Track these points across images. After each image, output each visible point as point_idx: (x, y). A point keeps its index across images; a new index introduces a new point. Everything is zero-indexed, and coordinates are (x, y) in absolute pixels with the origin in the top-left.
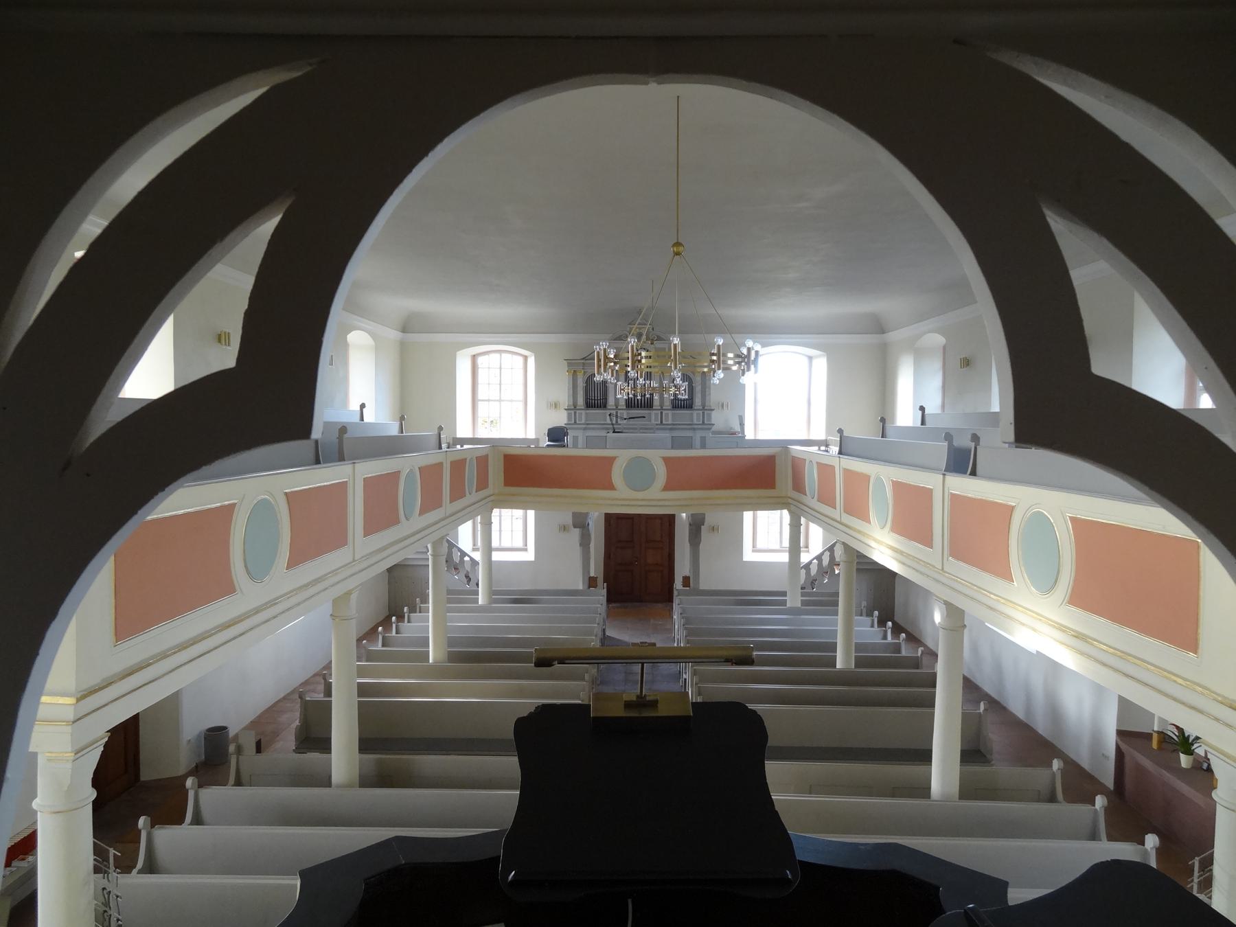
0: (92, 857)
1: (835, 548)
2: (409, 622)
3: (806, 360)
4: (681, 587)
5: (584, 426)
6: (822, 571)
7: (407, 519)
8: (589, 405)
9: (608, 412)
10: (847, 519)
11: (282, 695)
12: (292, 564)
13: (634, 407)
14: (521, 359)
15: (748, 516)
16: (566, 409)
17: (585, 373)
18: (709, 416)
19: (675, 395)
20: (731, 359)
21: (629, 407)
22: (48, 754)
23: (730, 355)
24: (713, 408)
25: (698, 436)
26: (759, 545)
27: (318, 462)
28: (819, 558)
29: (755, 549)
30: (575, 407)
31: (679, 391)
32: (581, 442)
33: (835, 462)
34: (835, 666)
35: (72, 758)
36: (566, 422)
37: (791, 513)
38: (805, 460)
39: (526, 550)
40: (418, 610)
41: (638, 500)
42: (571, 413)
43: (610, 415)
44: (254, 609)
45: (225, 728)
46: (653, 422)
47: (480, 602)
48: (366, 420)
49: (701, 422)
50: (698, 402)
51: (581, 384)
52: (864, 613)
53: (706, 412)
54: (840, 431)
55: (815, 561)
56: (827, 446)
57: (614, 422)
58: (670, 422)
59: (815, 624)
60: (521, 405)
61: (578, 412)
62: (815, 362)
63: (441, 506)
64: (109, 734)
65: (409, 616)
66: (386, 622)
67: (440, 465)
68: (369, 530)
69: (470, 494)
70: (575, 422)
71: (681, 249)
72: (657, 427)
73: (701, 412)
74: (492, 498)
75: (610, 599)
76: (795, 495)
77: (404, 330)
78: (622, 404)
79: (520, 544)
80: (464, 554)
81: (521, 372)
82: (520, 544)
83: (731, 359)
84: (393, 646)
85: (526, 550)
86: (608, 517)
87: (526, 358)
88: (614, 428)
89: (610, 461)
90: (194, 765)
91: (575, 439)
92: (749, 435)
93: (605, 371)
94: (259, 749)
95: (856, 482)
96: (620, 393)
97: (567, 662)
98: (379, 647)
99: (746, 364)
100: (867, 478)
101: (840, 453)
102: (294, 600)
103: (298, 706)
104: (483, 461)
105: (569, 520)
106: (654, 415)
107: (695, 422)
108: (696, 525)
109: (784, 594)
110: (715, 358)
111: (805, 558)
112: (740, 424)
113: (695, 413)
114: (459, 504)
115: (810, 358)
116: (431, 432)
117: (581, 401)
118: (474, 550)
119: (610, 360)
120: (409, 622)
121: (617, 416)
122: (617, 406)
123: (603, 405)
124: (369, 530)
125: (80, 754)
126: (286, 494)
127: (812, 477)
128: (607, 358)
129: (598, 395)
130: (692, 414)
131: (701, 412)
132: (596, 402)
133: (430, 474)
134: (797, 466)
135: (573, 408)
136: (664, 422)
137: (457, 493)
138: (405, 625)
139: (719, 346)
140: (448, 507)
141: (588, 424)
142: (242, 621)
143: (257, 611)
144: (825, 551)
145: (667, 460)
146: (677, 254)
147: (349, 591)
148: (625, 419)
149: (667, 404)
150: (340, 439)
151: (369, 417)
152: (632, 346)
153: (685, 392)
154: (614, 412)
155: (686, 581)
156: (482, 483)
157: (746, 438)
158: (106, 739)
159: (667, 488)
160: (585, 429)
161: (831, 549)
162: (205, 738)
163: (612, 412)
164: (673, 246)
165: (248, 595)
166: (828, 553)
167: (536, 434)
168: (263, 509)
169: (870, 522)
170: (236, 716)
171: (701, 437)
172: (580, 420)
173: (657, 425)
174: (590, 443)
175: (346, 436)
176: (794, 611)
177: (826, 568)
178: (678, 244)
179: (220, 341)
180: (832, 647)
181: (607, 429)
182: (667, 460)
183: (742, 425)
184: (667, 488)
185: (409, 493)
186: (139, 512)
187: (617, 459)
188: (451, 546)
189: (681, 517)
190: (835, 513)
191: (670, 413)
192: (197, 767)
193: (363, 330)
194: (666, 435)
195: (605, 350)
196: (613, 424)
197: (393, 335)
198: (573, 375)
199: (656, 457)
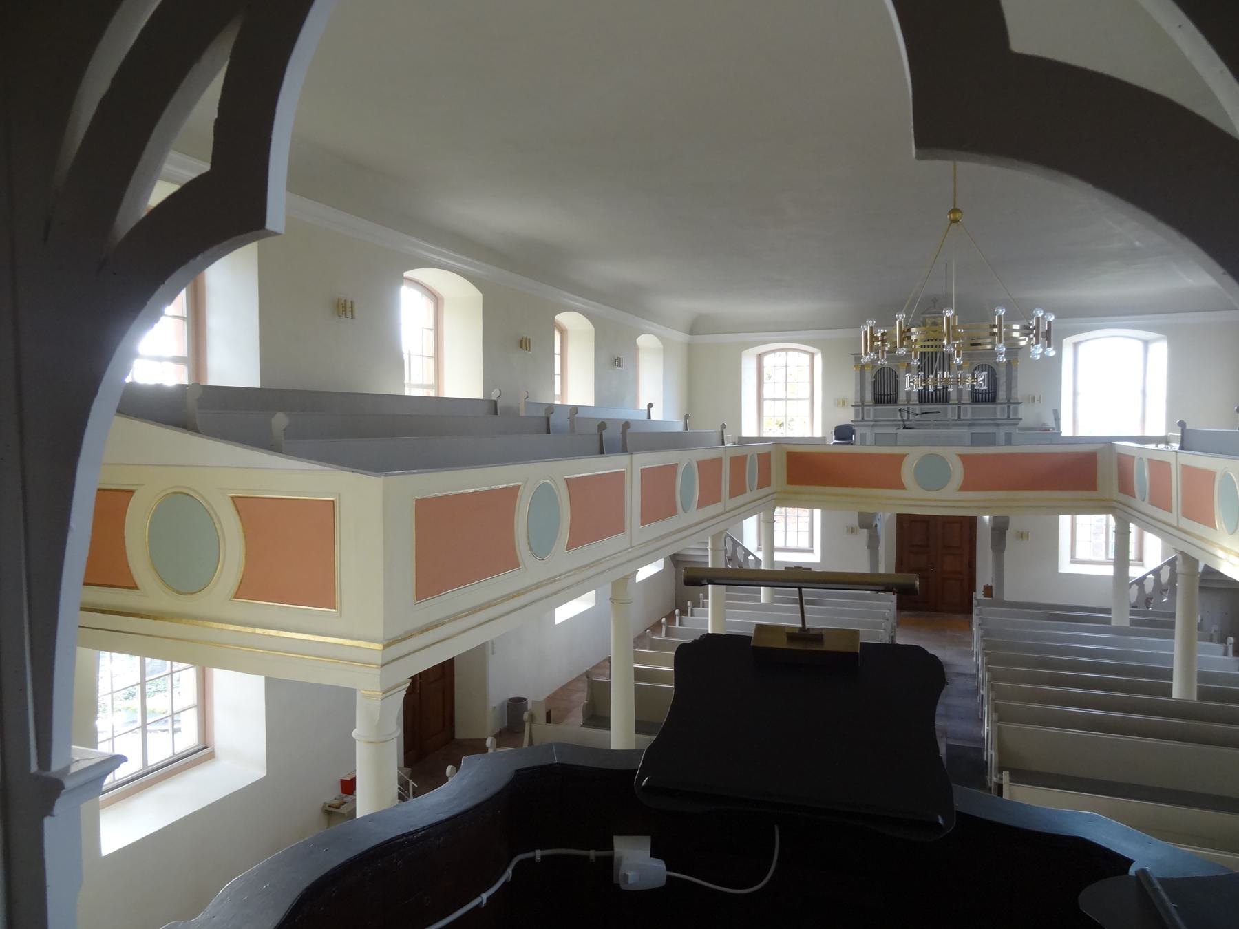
0: (397, 786)
2: (692, 615)
3: (1140, 345)
4: (982, 597)
6: (1159, 588)
7: (685, 511)
8: (878, 401)
9: (899, 408)
10: (1186, 524)
11: (575, 676)
12: (570, 546)
13: (928, 402)
14: (807, 357)
15: (1065, 521)
16: (852, 406)
17: (873, 368)
18: (1016, 411)
19: (973, 386)
20: (1016, 331)
21: (922, 402)
22: (364, 692)
23: (1016, 327)
24: (1019, 401)
25: (1001, 433)
26: (1080, 555)
27: (602, 452)
28: (1156, 572)
29: (1074, 560)
31: (977, 381)
32: (869, 439)
33: (1170, 459)
34: (1170, 695)
35: (380, 697)
36: (853, 419)
37: (1117, 519)
38: (1134, 457)
39: (812, 551)
40: (701, 604)
41: (930, 500)
42: (859, 410)
43: (900, 410)
44: (537, 583)
45: (524, 699)
46: (949, 416)
47: (762, 601)
48: (653, 418)
50: (1002, 394)
51: (869, 379)
52: (1215, 638)
53: (1012, 406)
54: (1182, 424)
55: (1151, 576)
57: (905, 418)
58: (969, 417)
59: (1145, 646)
60: (808, 403)
61: (865, 408)
62: (1153, 347)
63: (719, 501)
64: (411, 680)
65: (692, 610)
66: (671, 617)
67: (718, 462)
68: (645, 520)
69: (751, 491)
70: (863, 419)
71: (958, 215)
72: (954, 422)
73: (1006, 406)
74: (775, 496)
75: (901, 607)
76: (1122, 497)
77: (692, 332)
78: (915, 398)
79: (804, 544)
80: (748, 553)
81: (808, 370)
82: (806, 545)
83: (1016, 331)
84: (677, 638)
85: (812, 551)
86: (901, 519)
87: (812, 355)
89: (901, 458)
90: (499, 730)
91: (863, 436)
92: (1066, 430)
93: (871, 351)
94: (548, 720)
95: (1199, 483)
96: (910, 384)
97: (716, 581)
98: (663, 637)
99: (1035, 335)
100: (1209, 476)
101: (1182, 448)
102: (571, 580)
103: (584, 685)
104: (765, 459)
105: (855, 521)
106: (950, 411)
107: (999, 417)
108: (1000, 529)
109: (1108, 611)
110: (996, 330)
111: (1135, 572)
112: (1055, 420)
114: (739, 500)
115: (1146, 343)
116: (713, 430)
117: (869, 396)
118: (759, 549)
119: (877, 339)
120: (692, 615)
121: (908, 412)
122: (908, 400)
123: (892, 399)
124: (645, 520)
125: (389, 694)
126: (566, 479)
127: (1142, 477)
128: (875, 337)
129: (888, 390)
130: (995, 408)
131: (1006, 406)
132: (886, 397)
133: (709, 469)
134: (1124, 466)
135: (860, 404)
136: (962, 418)
137: (737, 489)
138: (688, 619)
139: (1000, 317)
140: (727, 502)
142: (523, 594)
143: (539, 586)
144: (1164, 564)
145: (964, 458)
146: (955, 221)
147: (626, 576)
148: (917, 414)
149: (966, 398)
150: (624, 433)
151: (656, 415)
152: (900, 322)
153: (984, 382)
154: (905, 408)
155: (988, 591)
156: (764, 481)
157: (1063, 435)
158: (408, 685)
159: (964, 487)
160: (873, 426)
161: (1172, 563)
162: (508, 707)
163: (902, 407)
164: (950, 212)
165: (530, 570)
166: (1167, 568)
168: (544, 493)
169: (1214, 527)
170: (536, 693)
171: (1006, 433)
172: (868, 416)
173: (953, 420)
174: (878, 440)
175: (629, 431)
176: (1119, 631)
177: (1163, 586)
178: (955, 210)
179: (521, 347)
180: (1168, 674)
181: (896, 425)
182: (964, 458)
183: (1057, 419)
184: (964, 487)
185: (687, 486)
186: (148, 303)
188: (736, 544)
189: (983, 521)
190: (1172, 518)
191: (969, 407)
192: (500, 732)
193: (653, 334)
194: (964, 431)
195: (871, 328)
196: (903, 421)
197: (680, 337)
198: (861, 370)
199: (952, 455)
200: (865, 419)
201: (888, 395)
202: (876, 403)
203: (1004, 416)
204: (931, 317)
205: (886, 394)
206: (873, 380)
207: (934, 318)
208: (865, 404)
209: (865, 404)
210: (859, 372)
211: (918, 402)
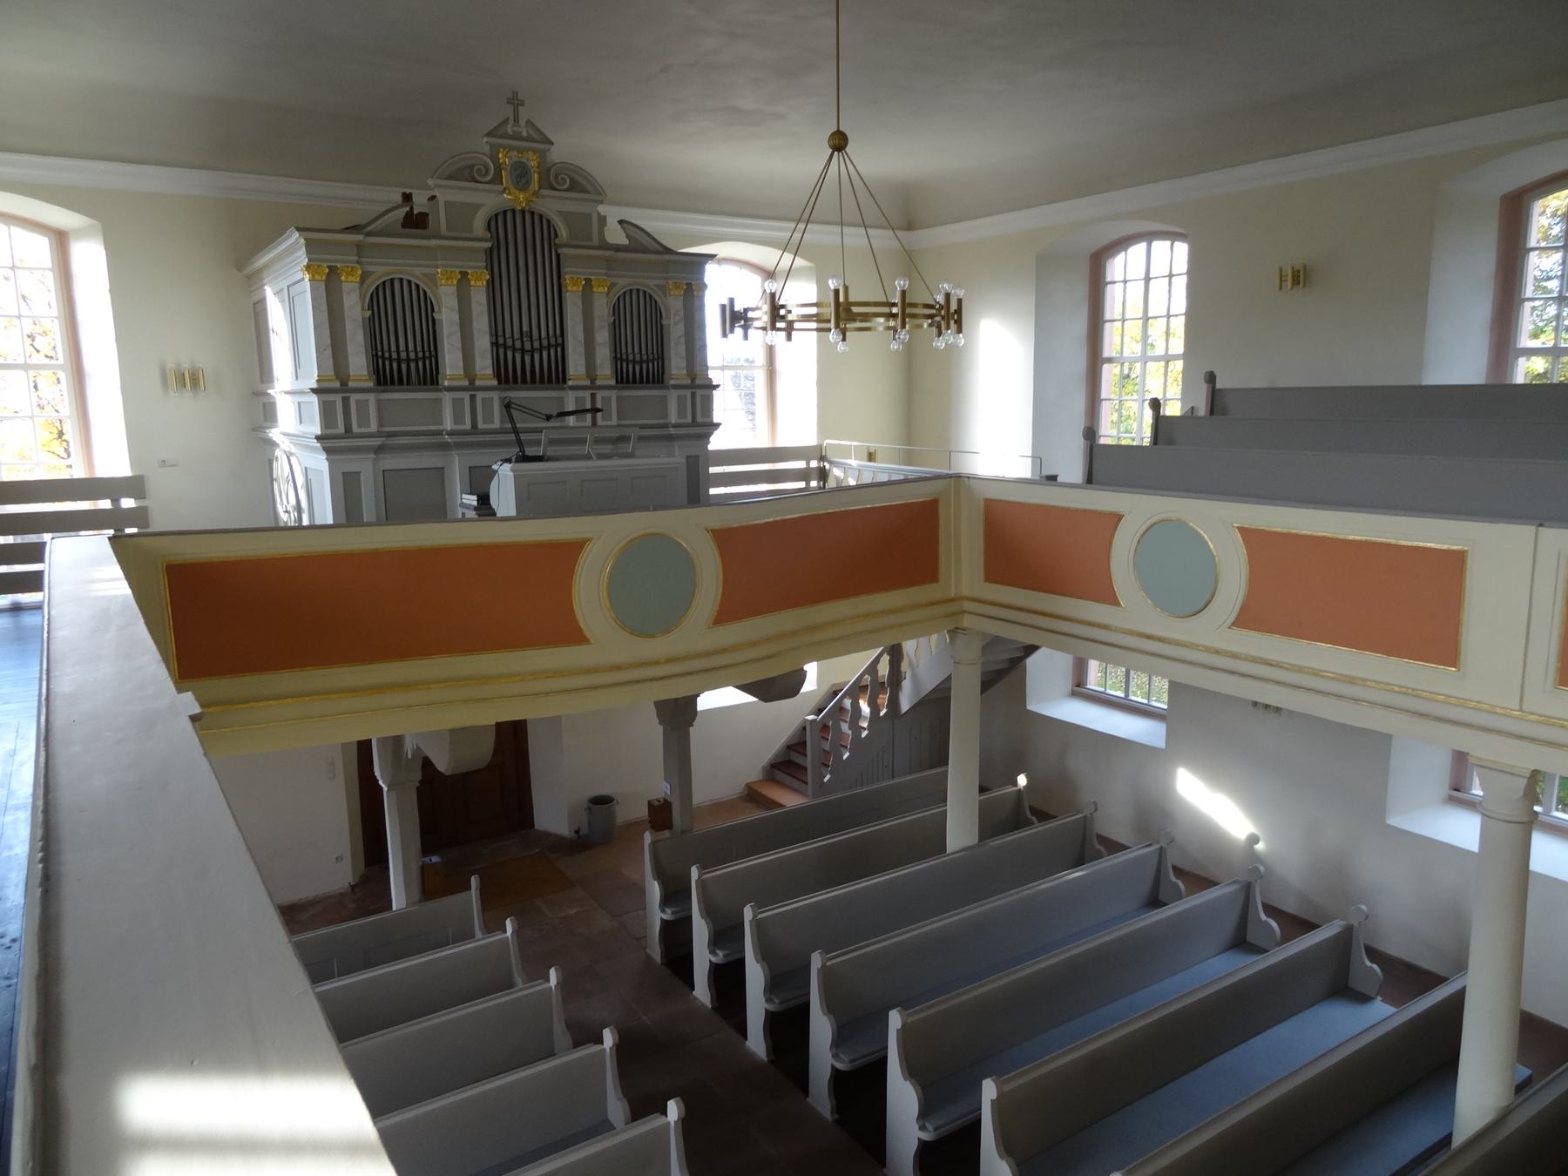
1: (879, 667)
8: (387, 375)
14: (38, 248)
17: (364, 276)
21: (507, 381)
49: (689, 420)
53: (699, 393)
56: (822, 458)
61: (354, 398)
70: (348, 429)
88: (520, 443)
89: (571, 551)
107: (673, 419)
113: (673, 396)
117: (358, 364)
131: (688, 393)
132: (404, 366)
141: (391, 435)
159: (726, 614)
160: (379, 450)
167: (134, 458)
172: (364, 421)
184: (726, 614)
187: (589, 547)
200: (355, 429)
201: (408, 360)
202: (378, 383)
203: (686, 417)
204: (511, 148)
205: (403, 355)
206: (370, 313)
207: (521, 151)
208: (351, 384)
209: (351, 384)
210: (323, 286)
211: (495, 382)
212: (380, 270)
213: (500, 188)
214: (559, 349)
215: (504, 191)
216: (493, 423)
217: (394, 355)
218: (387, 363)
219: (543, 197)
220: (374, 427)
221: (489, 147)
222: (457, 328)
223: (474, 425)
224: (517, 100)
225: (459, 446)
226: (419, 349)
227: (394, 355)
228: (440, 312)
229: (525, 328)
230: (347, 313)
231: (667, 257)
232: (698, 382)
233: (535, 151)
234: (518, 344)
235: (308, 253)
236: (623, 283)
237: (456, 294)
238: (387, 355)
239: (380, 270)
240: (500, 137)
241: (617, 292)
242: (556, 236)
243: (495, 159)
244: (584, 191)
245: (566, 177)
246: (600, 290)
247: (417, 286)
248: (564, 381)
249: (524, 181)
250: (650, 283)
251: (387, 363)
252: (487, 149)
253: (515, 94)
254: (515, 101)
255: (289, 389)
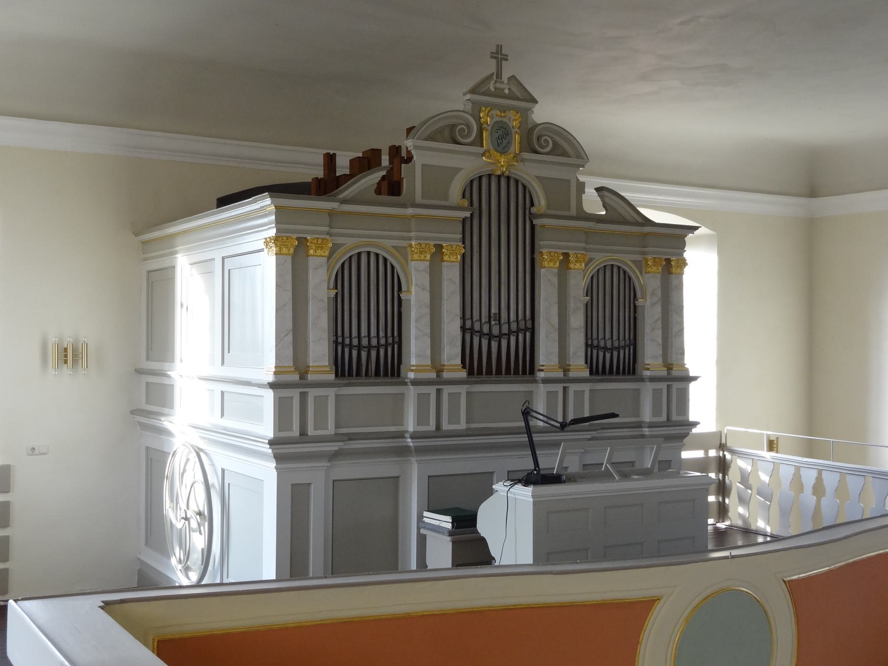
5: (334, 447)
30: (303, 376)
61: (312, 393)
107: (647, 420)
130: (637, 392)
141: (351, 437)
160: (334, 456)
172: (321, 422)
200: (311, 431)
201: (369, 347)
204: (494, 106)
206: (334, 292)
207: (504, 109)
209: (311, 377)
211: (463, 374)
212: (349, 242)
213: (480, 150)
214: (528, 334)
215: (483, 154)
216: (459, 423)
217: (355, 342)
218: (347, 350)
219: (523, 160)
220: (331, 430)
221: (471, 104)
222: (428, 310)
223: (438, 427)
224: (501, 54)
225: (420, 451)
226: (382, 334)
227: (355, 342)
228: (409, 291)
229: (494, 310)
230: (311, 291)
231: (647, 229)
232: (675, 373)
233: (517, 110)
234: (486, 329)
235: (278, 222)
236: (601, 259)
237: (428, 269)
238: (347, 341)
239: (349, 242)
240: (484, 94)
241: (592, 268)
242: (532, 204)
243: (478, 119)
244: (565, 154)
245: (549, 140)
246: (576, 266)
247: (385, 260)
248: (532, 372)
249: (505, 142)
250: (626, 259)
251: (347, 350)
252: (469, 107)
253: (499, 48)
254: (499, 56)
255: (204, 374)
